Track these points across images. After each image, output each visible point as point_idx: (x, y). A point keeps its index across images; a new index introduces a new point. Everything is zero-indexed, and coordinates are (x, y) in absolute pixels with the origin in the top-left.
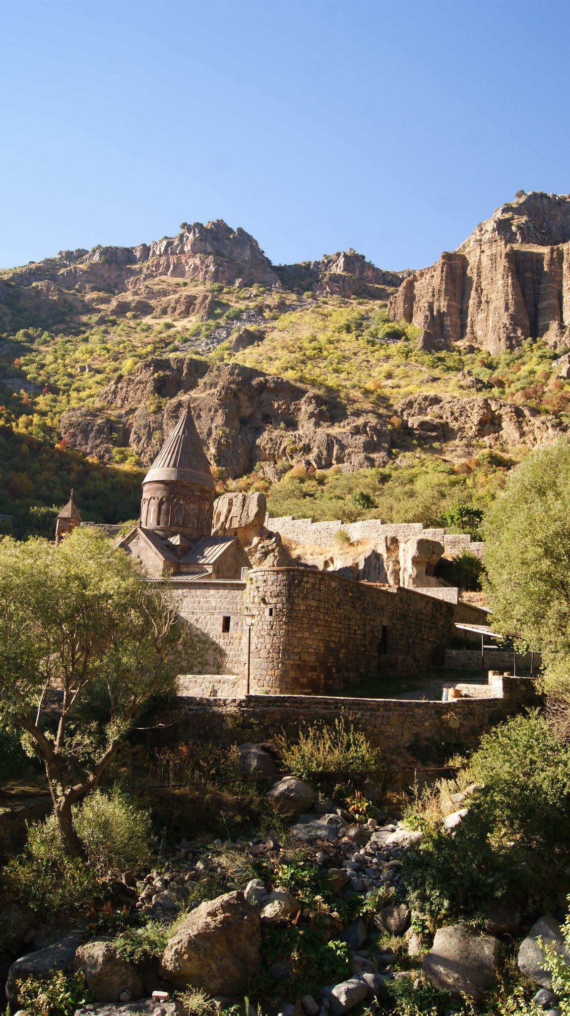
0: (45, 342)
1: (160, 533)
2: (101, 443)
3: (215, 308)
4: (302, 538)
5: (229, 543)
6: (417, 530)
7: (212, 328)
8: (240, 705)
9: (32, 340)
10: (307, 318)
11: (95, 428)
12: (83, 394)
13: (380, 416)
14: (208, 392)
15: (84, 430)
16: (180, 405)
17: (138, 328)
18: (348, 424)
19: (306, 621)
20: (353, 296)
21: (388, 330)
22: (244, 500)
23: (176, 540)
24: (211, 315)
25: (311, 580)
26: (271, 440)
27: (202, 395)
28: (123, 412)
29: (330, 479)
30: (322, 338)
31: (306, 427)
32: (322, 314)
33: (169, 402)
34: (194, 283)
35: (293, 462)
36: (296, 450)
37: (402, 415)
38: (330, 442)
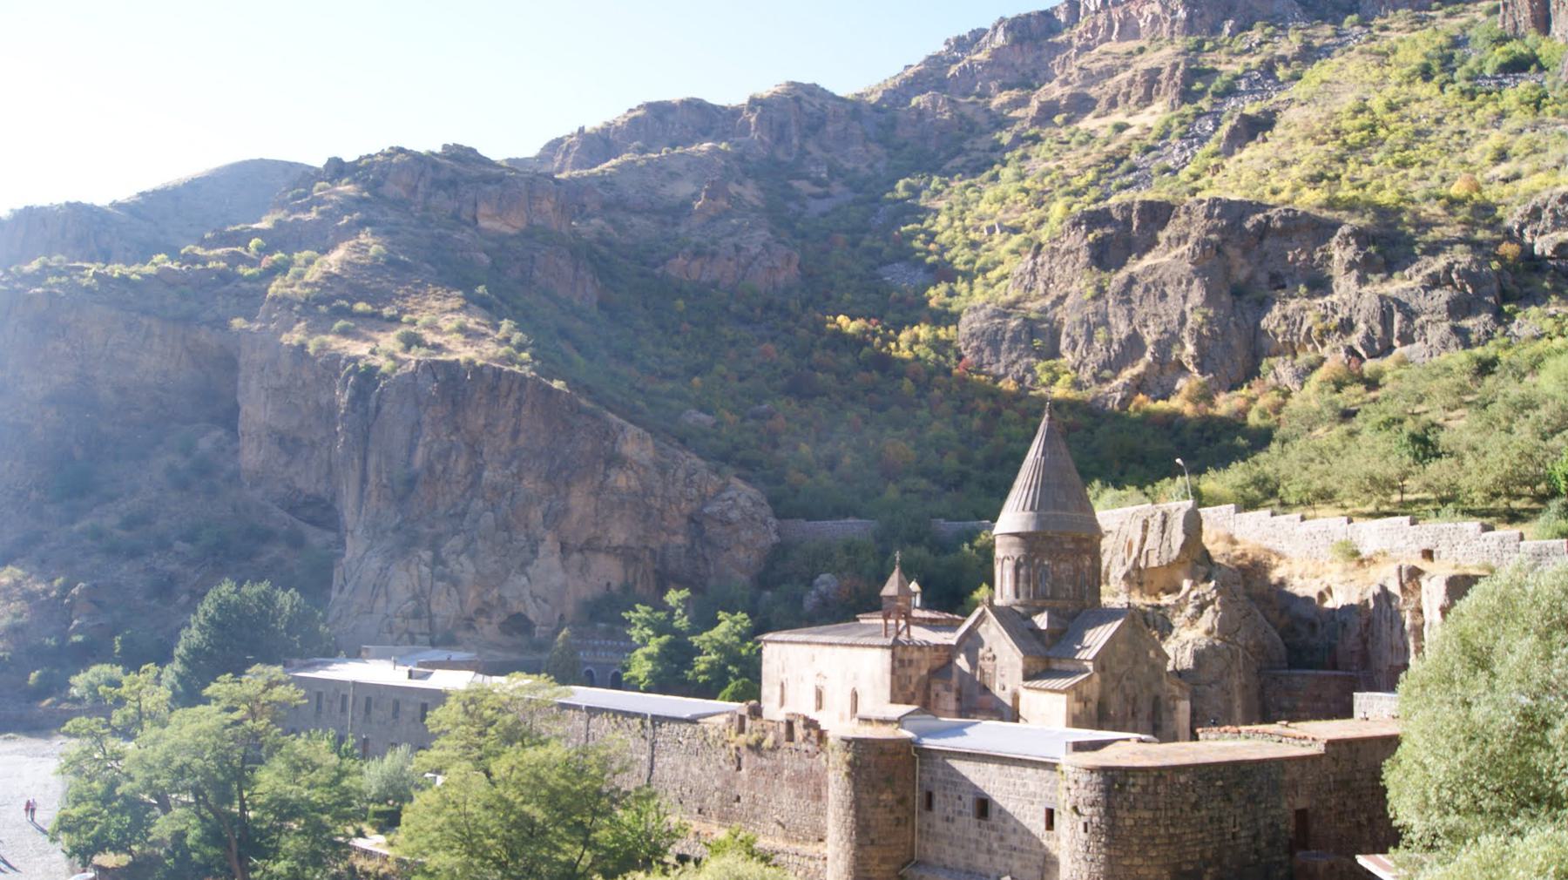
0: (938, 192)
1: (1021, 610)
2: (1020, 357)
3: (1192, 81)
4: (1286, 548)
5: (1119, 623)
6: (1471, 534)
7: (1190, 120)
9: (915, 192)
10: (1351, 68)
11: (1008, 336)
13: (1476, 246)
14: (1174, 252)
15: (993, 340)
16: (1132, 280)
17: (1074, 141)
18: (1418, 271)
19: (1135, 840)
20: (1436, 5)
21: (1502, 59)
22: (1164, 523)
23: (1041, 621)
24: (1187, 96)
25: (1140, 781)
26: (1285, 317)
27: (1166, 259)
28: (1048, 303)
29: (1389, 377)
30: (1377, 103)
31: (1345, 286)
32: (1378, 54)
34: (1155, 45)
35: (1324, 352)
36: (1328, 331)
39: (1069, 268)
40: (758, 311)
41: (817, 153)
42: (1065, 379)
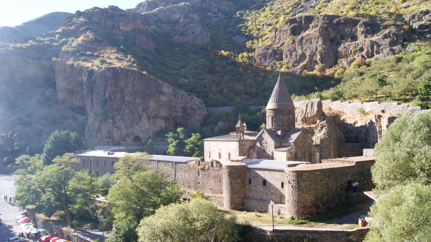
0: (248, 15)
1: (273, 130)
2: (272, 60)
4: (345, 111)
5: (300, 132)
6: (395, 106)
8: (270, 232)
9: (242, 15)
11: (268, 55)
12: (264, 38)
13: (397, 26)
14: (314, 30)
15: (264, 56)
16: (302, 38)
18: (381, 34)
19: (305, 190)
22: (312, 105)
23: (279, 133)
25: (306, 174)
26: (345, 47)
27: (312, 32)
28: (279, 45)
29: (373, 63)
31: (361, 38)
33: (298, 37)
36: (356, 51)
37: (409, 23)
38: (373, 44)
39: (285, 35)
40: (199, 50)
41: (214, 4)
42: (284, 66)
